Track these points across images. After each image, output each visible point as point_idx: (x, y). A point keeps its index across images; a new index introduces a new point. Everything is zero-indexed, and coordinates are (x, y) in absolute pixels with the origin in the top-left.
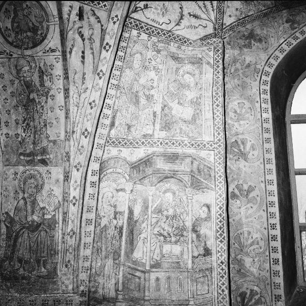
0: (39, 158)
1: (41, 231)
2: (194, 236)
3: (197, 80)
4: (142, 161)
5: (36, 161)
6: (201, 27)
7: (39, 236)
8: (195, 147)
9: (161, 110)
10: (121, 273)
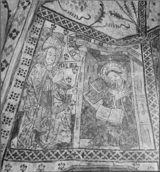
3: (125, 79)
6: (124, 27)
8: (131, 159)
9: (80, 112)
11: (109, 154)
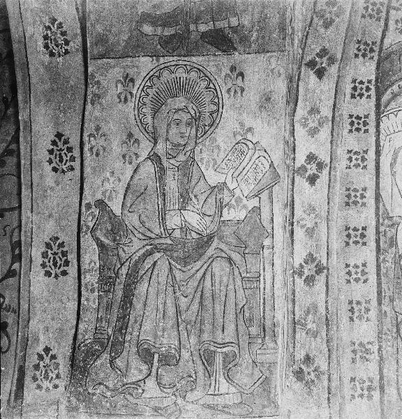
0: (203, 28)
1: (213, 259)
7: (208, 277)
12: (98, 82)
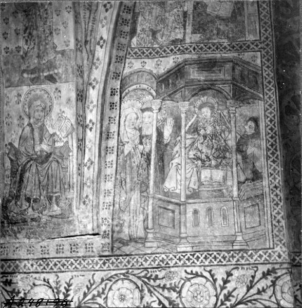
0: (45, 74)
1: (52, 161)
2: (239, 157)
4: (171, 72)
5: (42, 78)
7: (50, 169)
8: (237, 50)
10: (150, 208)
11: (217, 46)
12: (8, 97)
